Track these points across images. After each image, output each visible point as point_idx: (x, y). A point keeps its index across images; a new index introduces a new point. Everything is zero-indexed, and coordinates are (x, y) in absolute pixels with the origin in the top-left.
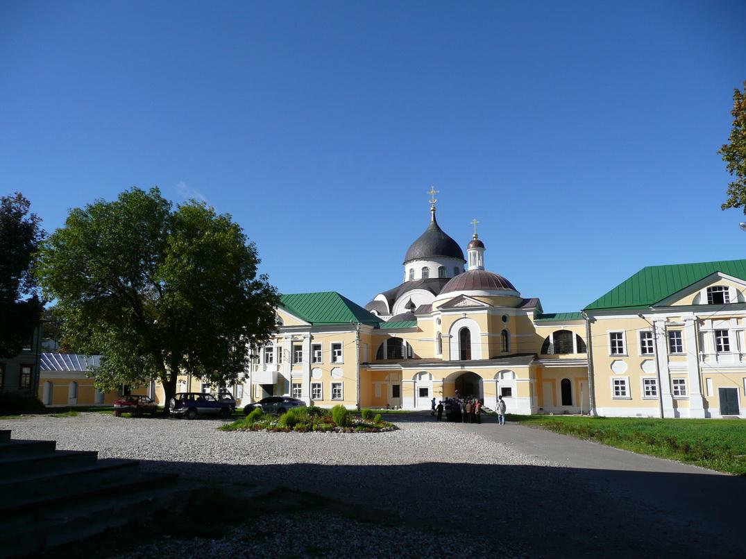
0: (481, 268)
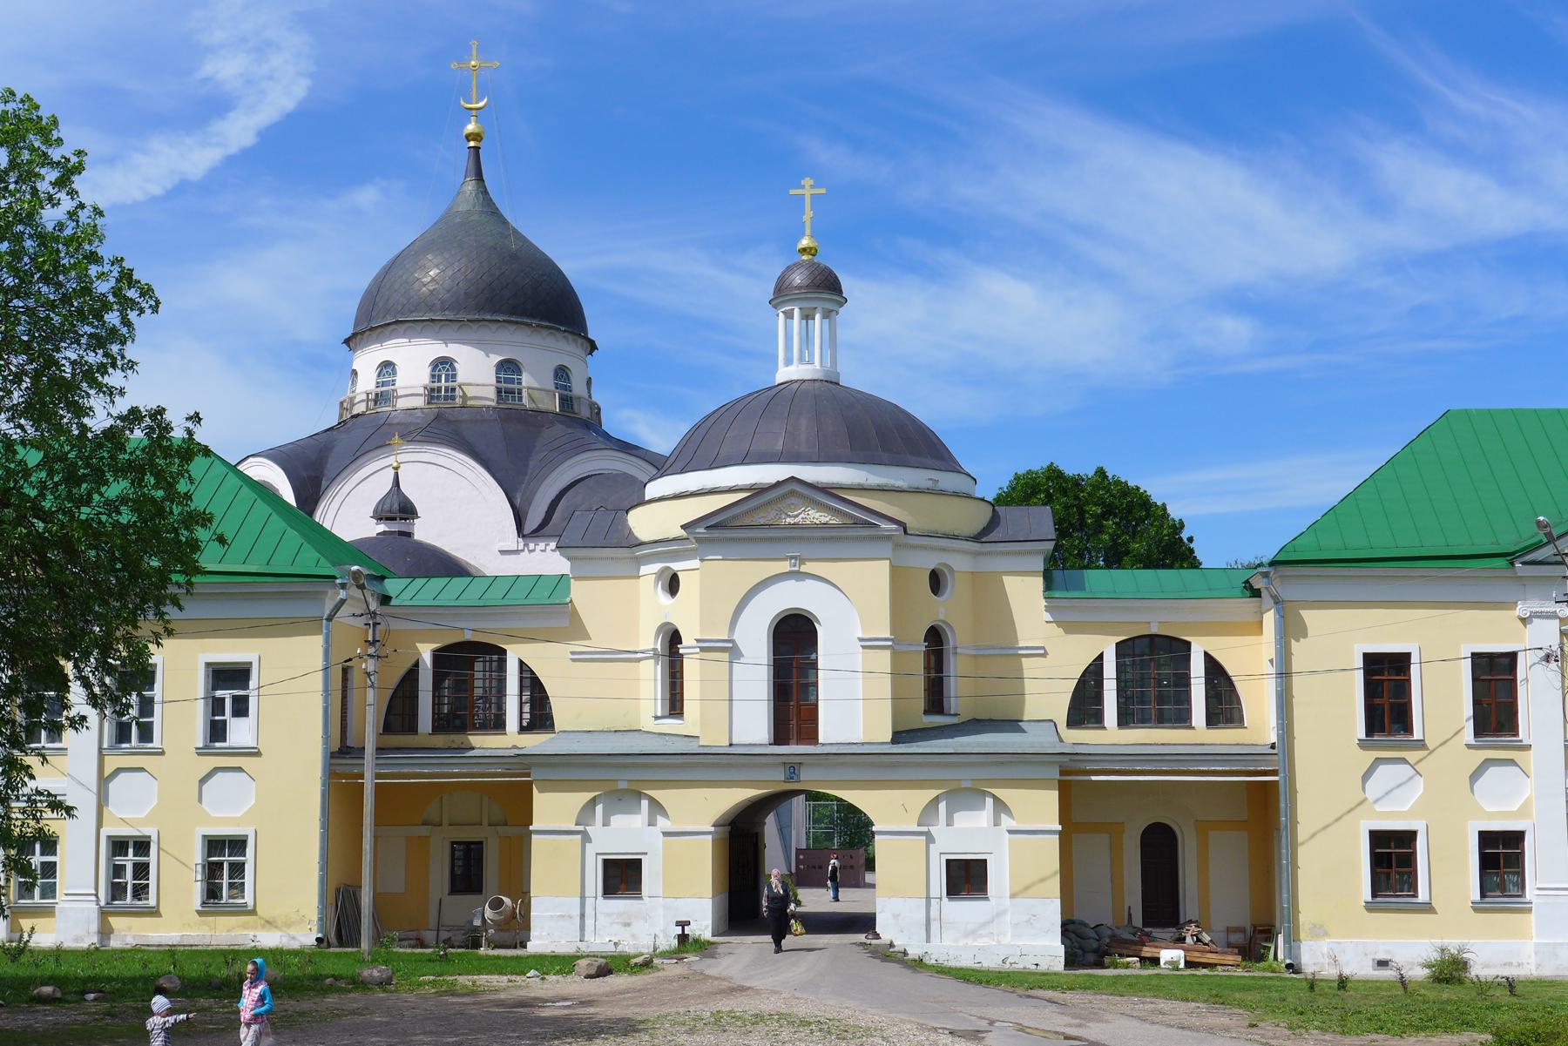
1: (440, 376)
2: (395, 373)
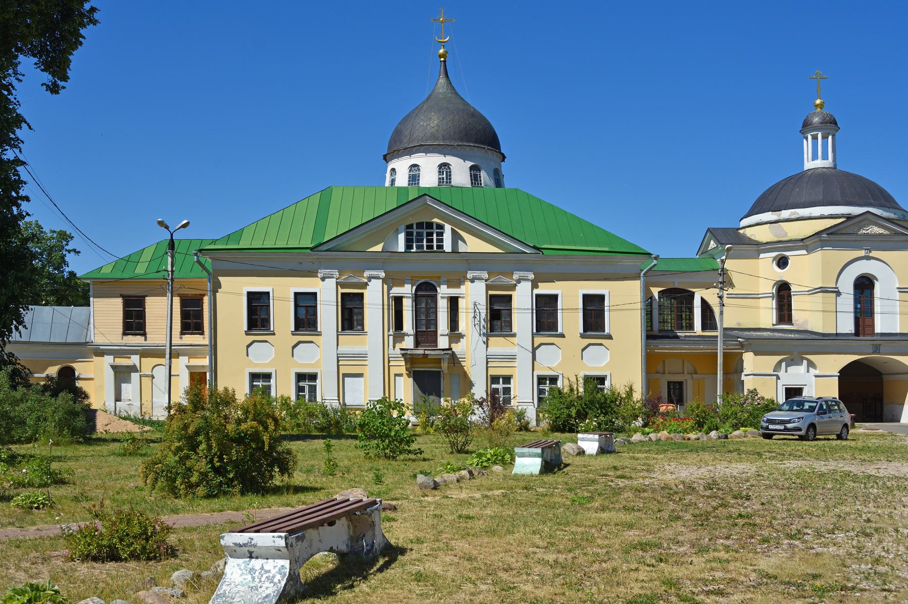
0: (835, 167)
1: (443, 172)
2: (419, 170)
